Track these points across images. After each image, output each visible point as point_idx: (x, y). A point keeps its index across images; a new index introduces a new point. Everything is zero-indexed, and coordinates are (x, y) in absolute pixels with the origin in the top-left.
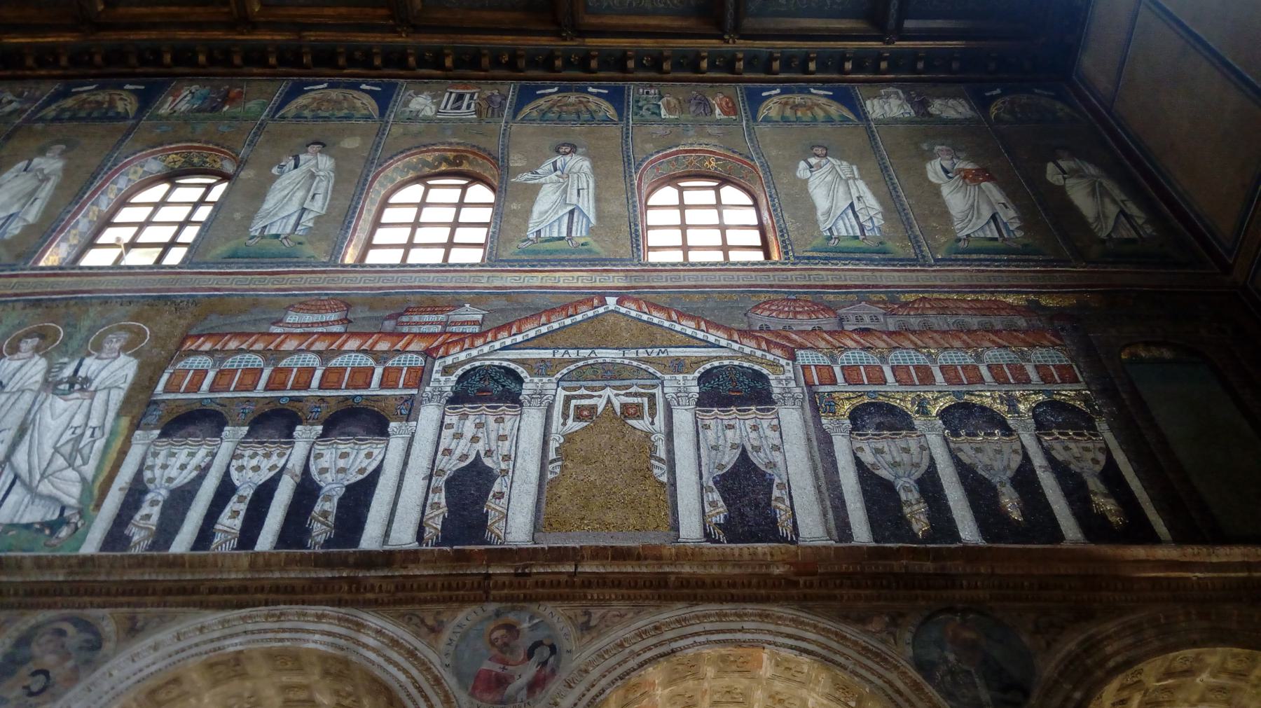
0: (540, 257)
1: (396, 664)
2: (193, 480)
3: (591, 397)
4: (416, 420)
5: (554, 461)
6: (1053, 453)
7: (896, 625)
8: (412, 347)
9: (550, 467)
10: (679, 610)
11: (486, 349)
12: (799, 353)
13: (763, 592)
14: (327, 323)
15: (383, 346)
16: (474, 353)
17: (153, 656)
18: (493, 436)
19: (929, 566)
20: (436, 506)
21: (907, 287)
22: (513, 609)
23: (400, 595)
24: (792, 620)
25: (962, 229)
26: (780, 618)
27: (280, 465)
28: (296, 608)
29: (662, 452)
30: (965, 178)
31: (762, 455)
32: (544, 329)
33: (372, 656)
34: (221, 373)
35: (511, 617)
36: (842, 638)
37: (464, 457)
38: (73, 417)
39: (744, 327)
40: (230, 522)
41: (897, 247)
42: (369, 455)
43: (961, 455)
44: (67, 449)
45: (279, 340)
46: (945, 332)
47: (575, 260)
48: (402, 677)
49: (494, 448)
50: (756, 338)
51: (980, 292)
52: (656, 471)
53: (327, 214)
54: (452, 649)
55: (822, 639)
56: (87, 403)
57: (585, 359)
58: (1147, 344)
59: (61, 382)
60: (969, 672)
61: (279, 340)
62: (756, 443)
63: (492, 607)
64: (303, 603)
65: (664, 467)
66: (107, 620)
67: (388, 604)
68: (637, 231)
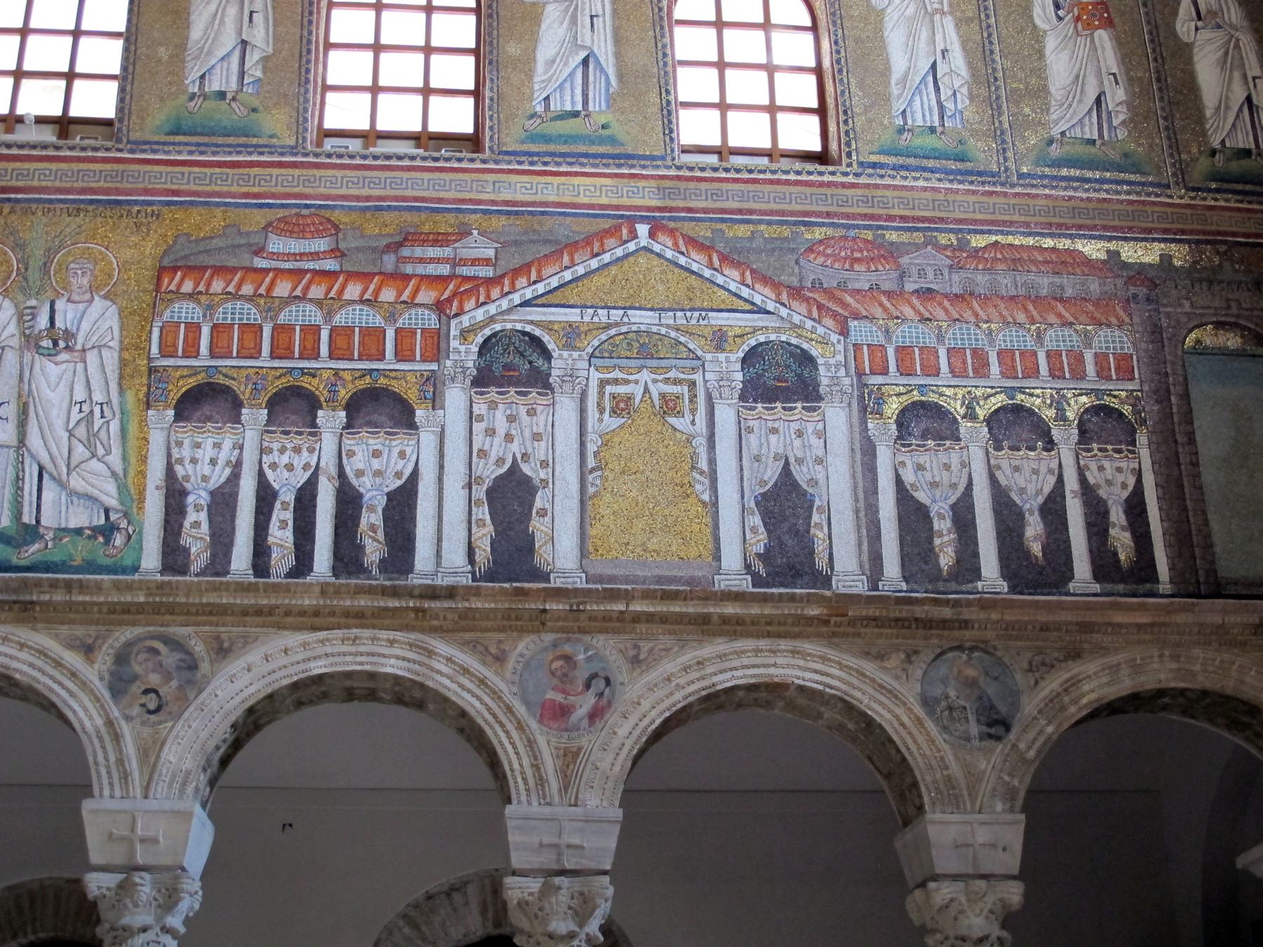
0: (551, 148)
1: (469, 691)
2: (228, 480)
3: (627, 382)
4: (443, 408)
5: (593, 470)
6: (1087, 474)
7: (911, 662)
8: (420, 299)
9: (590, 478)
10: (720, 646)
11: (505, 304)
12: (853, 324)
13: (796, 629)
14: (315, 256)
15: (388, 295)
16: (492, 309)
17: (247, 677)
18: (527, 434)
19: (947, 613)
20: (481, 523)
21: (982, 222)
22: (568, 640)
23: (463, 623)
24: (821, 657)
25: (1056, 122)
26: (809, 655)
27: (313, 463)
28: (367, 633)
29: (703, 464)
30: (1078, 19)
31: (805, 469)
32: (568, 276)
33: (447, 682)
34: (215, 327)
35: (568, 649)
36: (861, 674)
37: (500, 461)
38: (72, 391)
39: (795, 282)
40: (281, 536)
41: (982, 152)
42: (402, 455)
43: (999, 475)
44: (81, 432)
45: (268, 280)
46: (1012, 298)
47: (595, 156)
48: (477, 704)
49: (530, 451)
50: (807, 300)
51: (1060, 236)
52: (698, 487)
53: (277, 51)
54: (517, 678)
55: (843, 675)
56: (80, 366)
57: (617, 324)
58: (1219, 325)
59: (39, 337)
60: (965, 708)
61: (268, 280)
62: (800, 454)
63: (549, 637)
64: (374, 627)
65: (707, 482)
66: (196, 638)
67: (452, 631)
68: (668, 102)
